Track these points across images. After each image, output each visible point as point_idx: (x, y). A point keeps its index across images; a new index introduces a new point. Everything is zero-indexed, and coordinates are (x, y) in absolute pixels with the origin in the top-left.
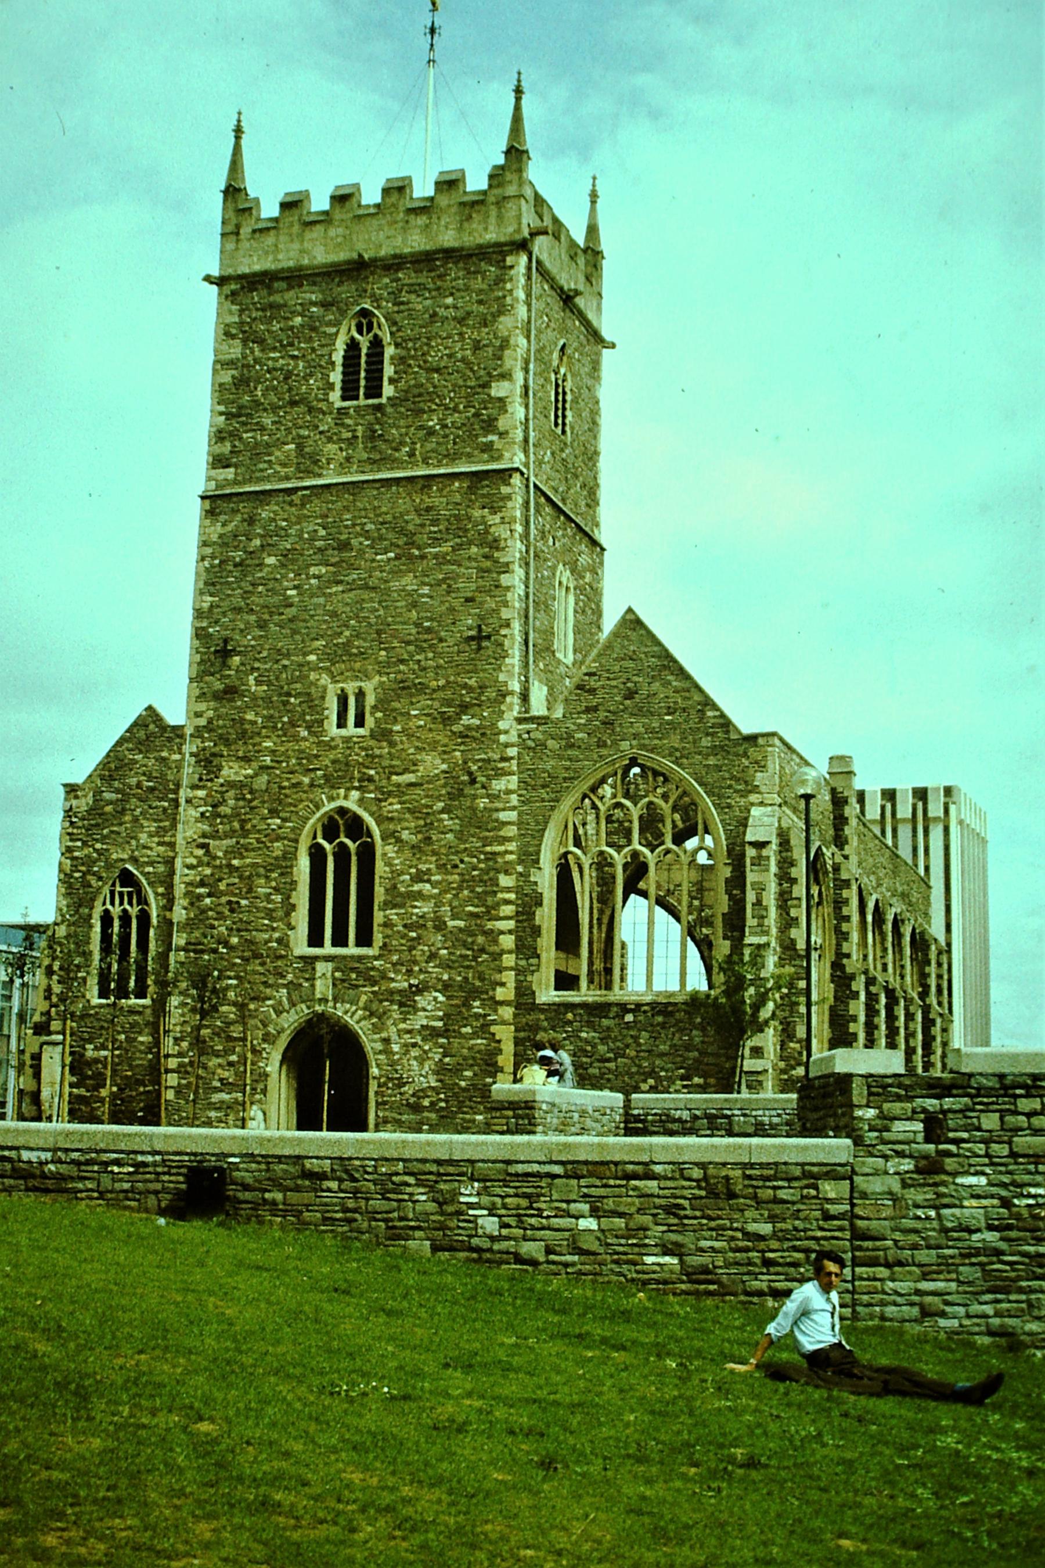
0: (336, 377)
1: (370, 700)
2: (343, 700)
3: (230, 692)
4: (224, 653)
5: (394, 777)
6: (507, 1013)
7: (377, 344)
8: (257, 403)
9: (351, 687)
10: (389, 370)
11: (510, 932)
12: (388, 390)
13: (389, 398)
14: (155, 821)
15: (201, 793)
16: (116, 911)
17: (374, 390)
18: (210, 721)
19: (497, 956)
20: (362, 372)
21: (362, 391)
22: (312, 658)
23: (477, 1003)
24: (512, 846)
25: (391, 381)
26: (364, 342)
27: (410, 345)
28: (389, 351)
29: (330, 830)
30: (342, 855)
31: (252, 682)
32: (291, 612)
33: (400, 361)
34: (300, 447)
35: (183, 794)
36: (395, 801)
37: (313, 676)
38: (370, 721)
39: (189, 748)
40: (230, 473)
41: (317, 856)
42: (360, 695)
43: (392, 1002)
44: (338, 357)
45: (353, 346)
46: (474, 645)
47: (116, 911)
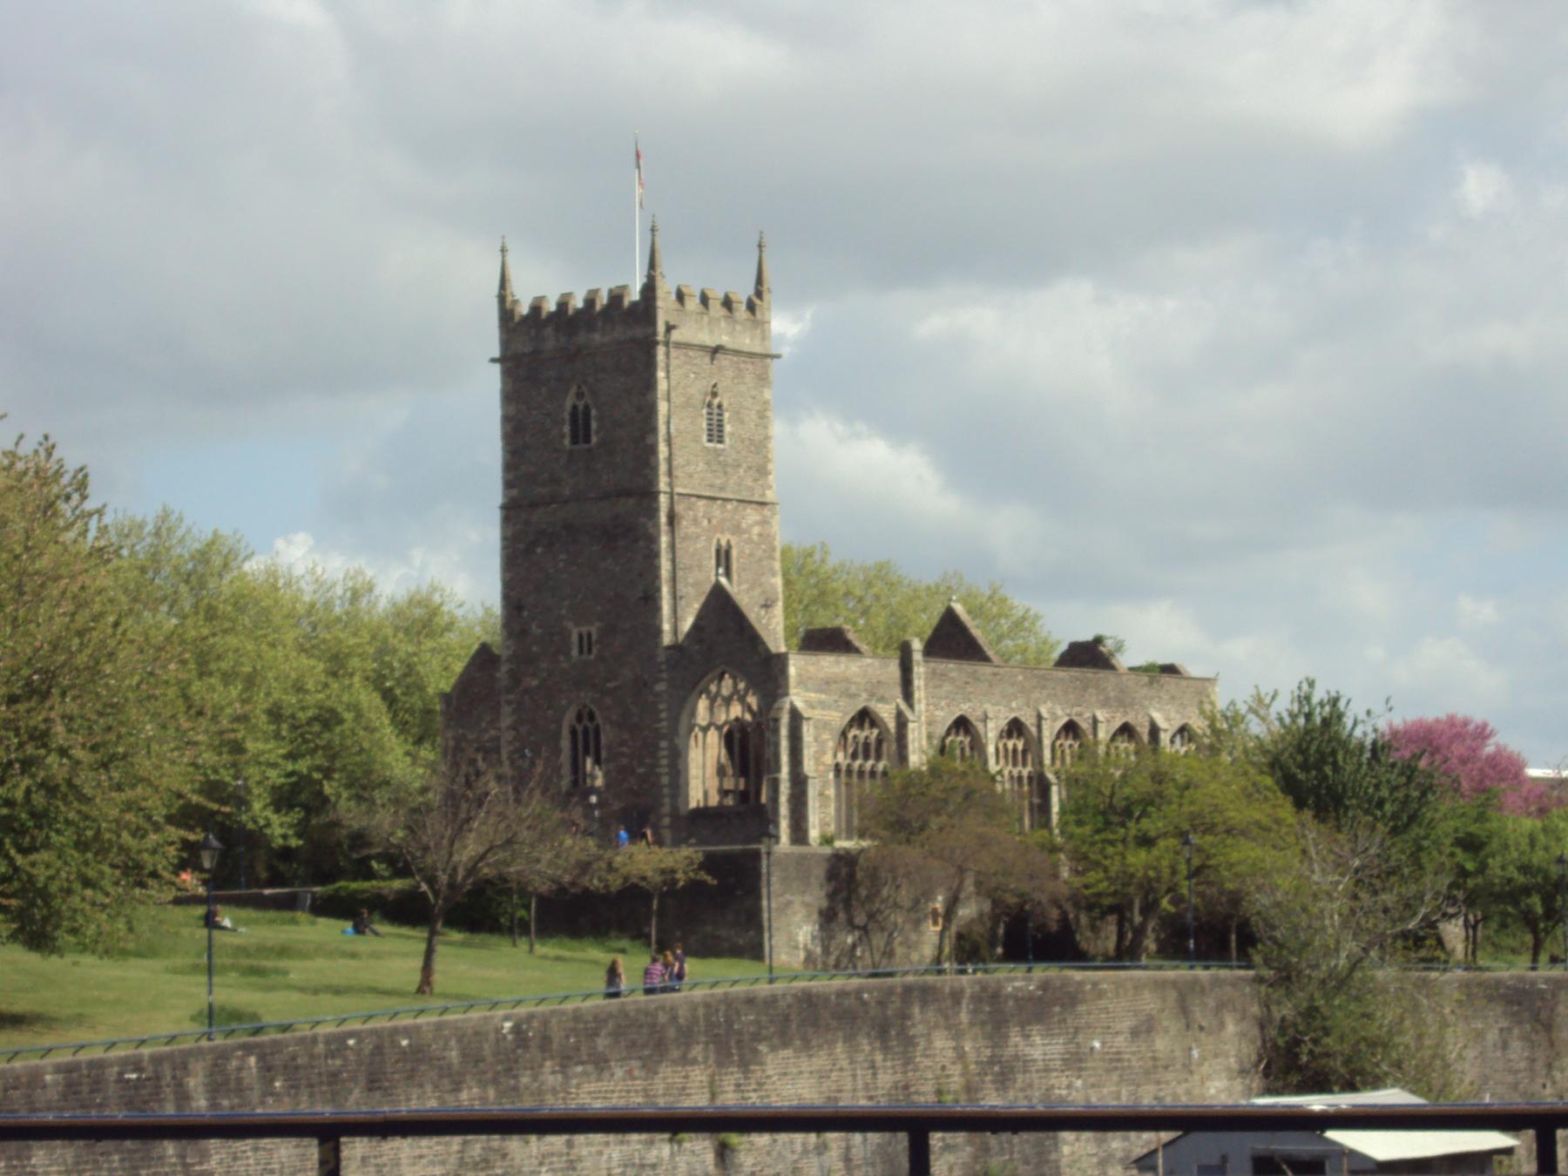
0: (567, 429)
1: (594, 638)
2: (581, 637)
7: (587, 408)
10: (594, 425)
12: (594, 439)
15: (511, 697)
17: (587, 440)
20: (581, 430)
25: (597, 433)
28: (593, 412)
29: (579, 718)
30: (586, 731)
38: (594, 650)
41: (574, 732)
42: (589, 635)
44: (567, 416)
45: (575, 407)
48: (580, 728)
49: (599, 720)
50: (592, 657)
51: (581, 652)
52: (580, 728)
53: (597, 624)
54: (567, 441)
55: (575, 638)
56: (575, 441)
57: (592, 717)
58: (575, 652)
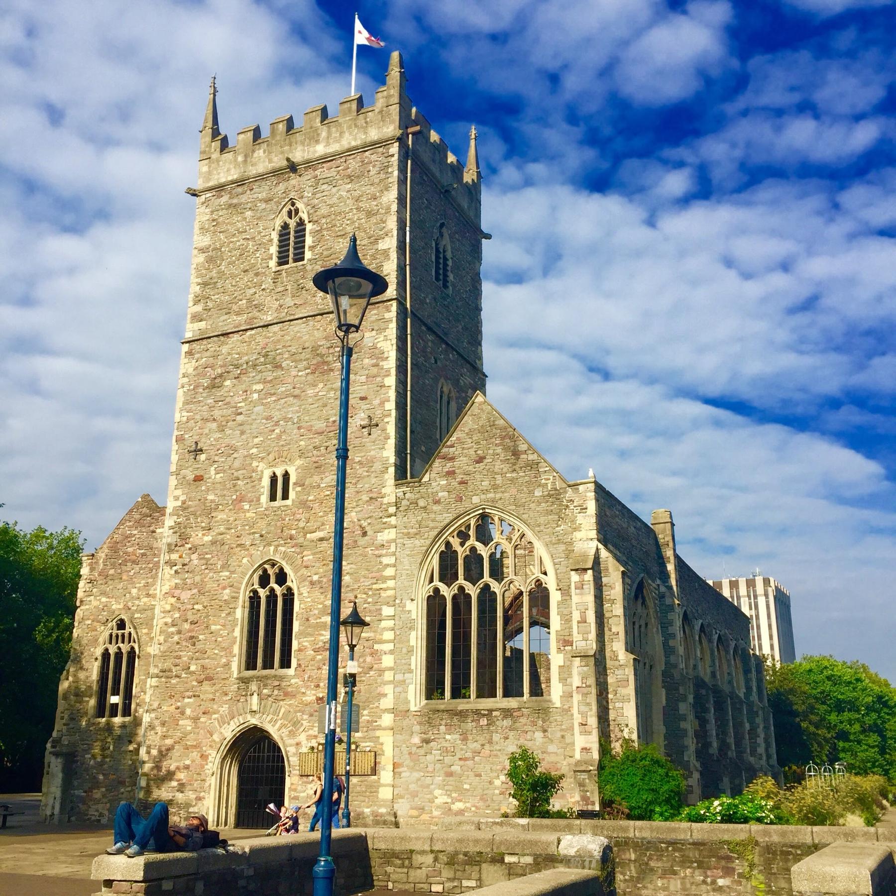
1: (292, 480)
3: (198, 479)
4: (198, 451)
5: (308, 536)
6: (387, 720)
7: (301, 223)
8: (221, 273)
9: (279, 473)
10: (309, 240)
11: (391, 652)
12: (308, 255)
13: (309, 260)
14: (143, 579)
16: (112, 650)
18: (184, 502)
19: (381, 671)
21: (291, 255)
22: (254, 451)
23: (365, 712)
24: (391, 583)
26: (292, 223)
27: (324, 221)
28: (309, 227)
29: (264, 580)
31: (213, 472)
32: (240, 418)
33: (314, 233)
34: (249, 301)
35: (164, 557)
36: (309, 552)
37: (255, 464)
38: (292, 494)
39: (169, 522)
40: (202, 325)
41: (254, 599)
42: (286, 476)
43: (303, 712)
44: (275, 236)
45: (285, 226)
46: (365, 431)
47: (112, 650)
48: (263, 593)
49: (292, 581)
50: (288, 502)
51: (273, 498)
52: (263, 593)
53: (299, 462)
54: (273, 263)
55: (266, 482)
56: (283, 260)
57: (282, 578)
58: (265, 498)
